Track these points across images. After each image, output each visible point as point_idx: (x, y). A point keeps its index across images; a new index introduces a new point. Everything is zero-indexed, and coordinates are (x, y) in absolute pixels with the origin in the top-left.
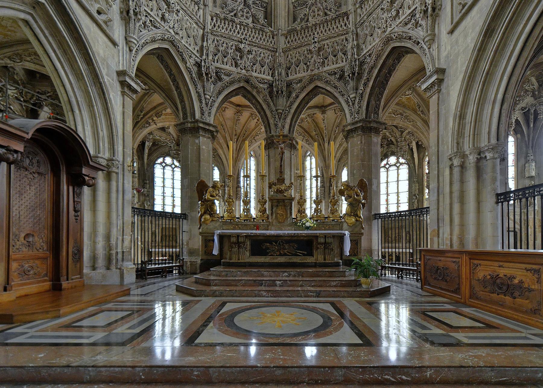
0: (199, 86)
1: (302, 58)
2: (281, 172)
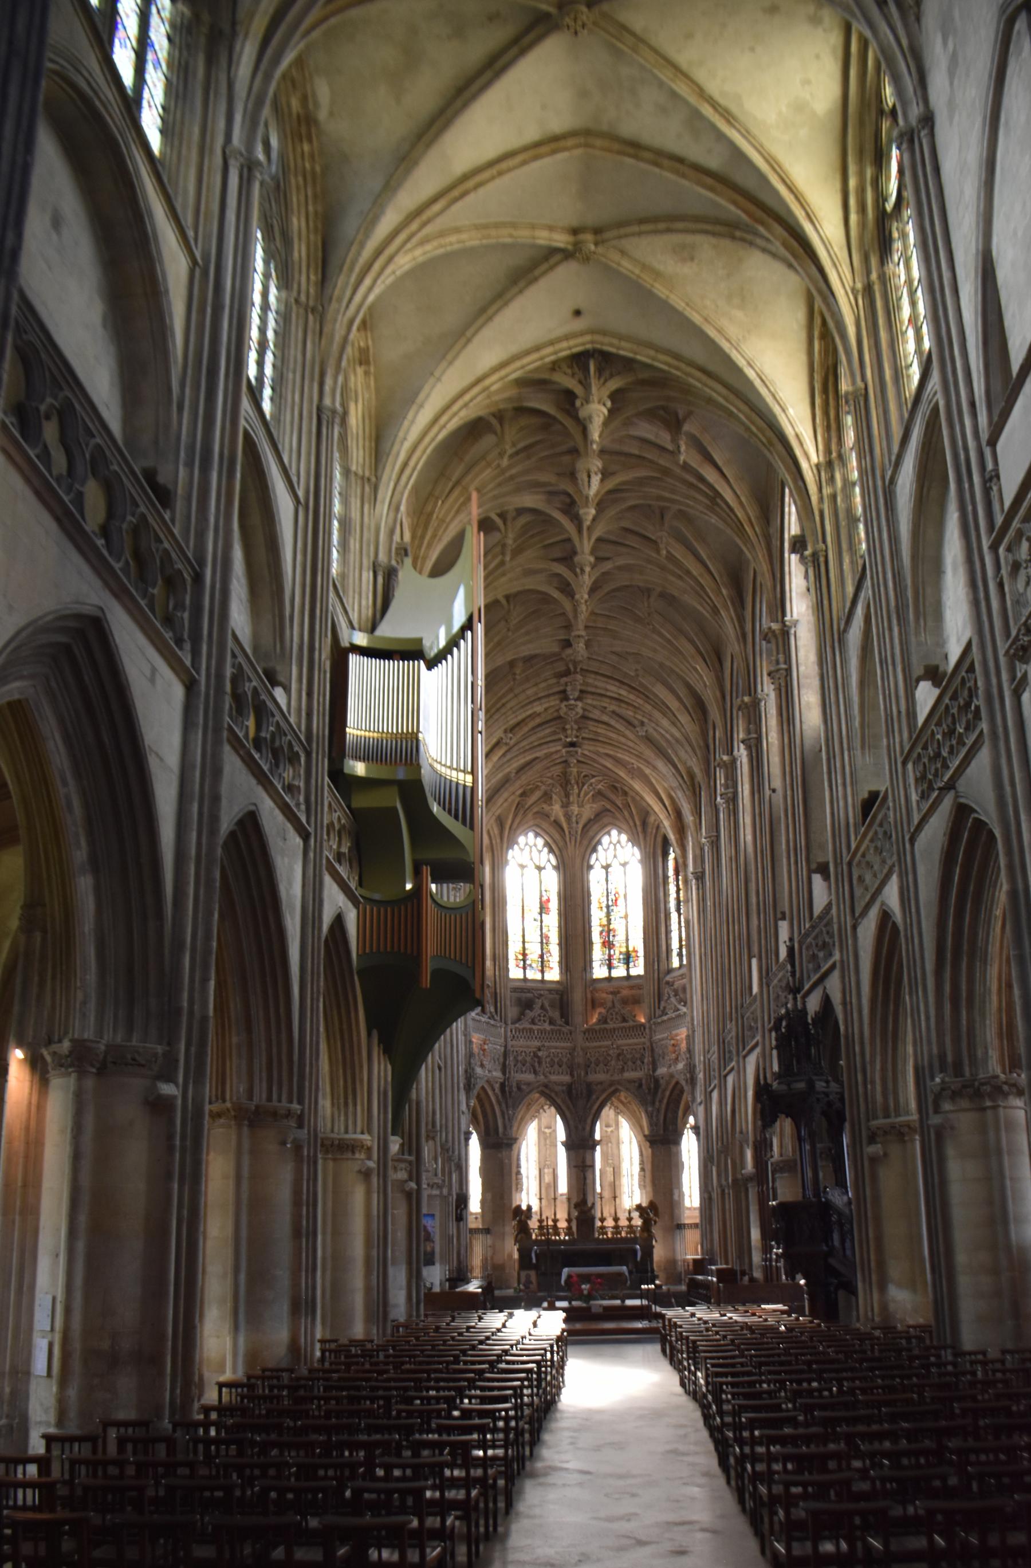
0: (504, 1105)
1: (601, 1059)
2: (585, 1194)
